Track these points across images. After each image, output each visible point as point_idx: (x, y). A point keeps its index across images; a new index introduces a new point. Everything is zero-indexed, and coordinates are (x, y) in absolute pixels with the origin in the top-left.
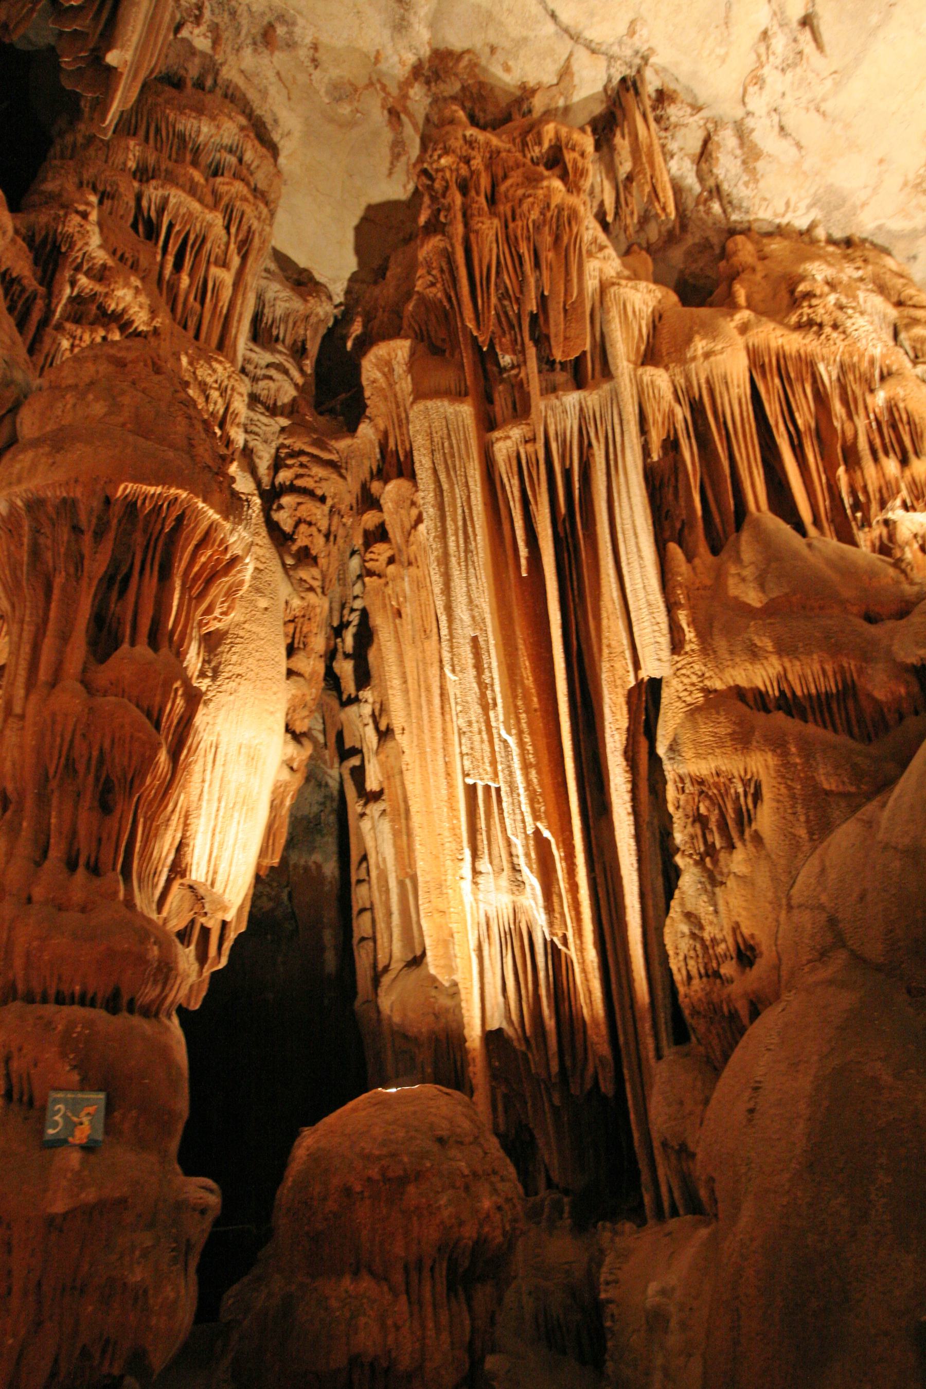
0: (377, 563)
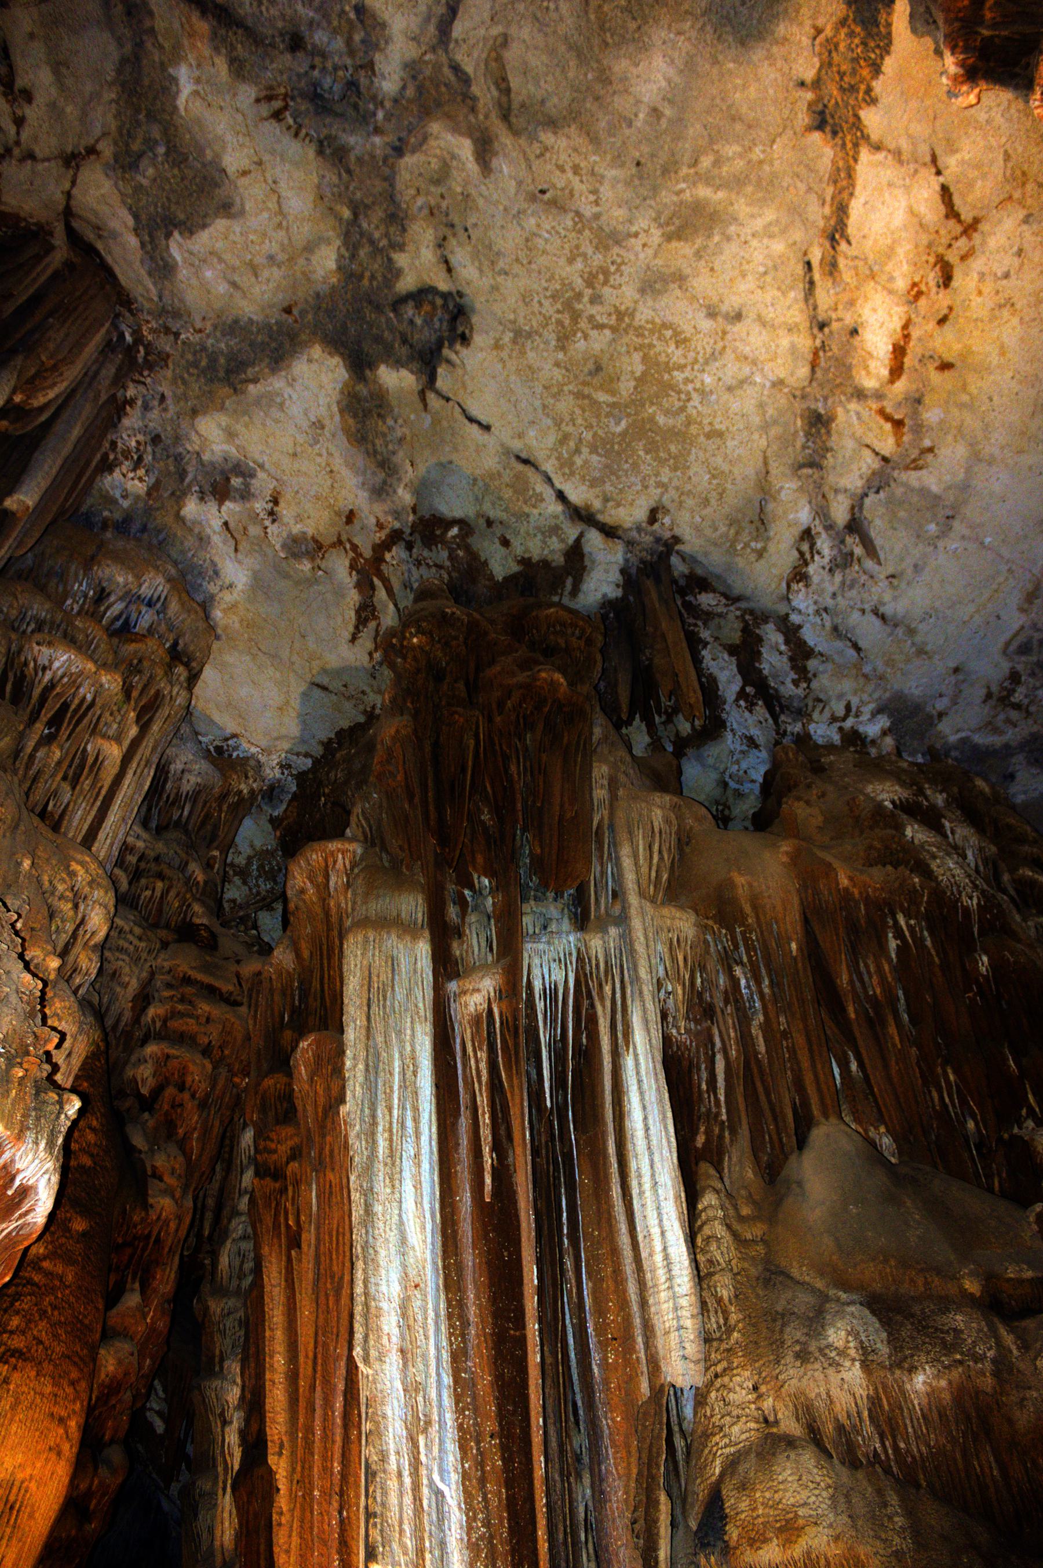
0: (275, 1157)
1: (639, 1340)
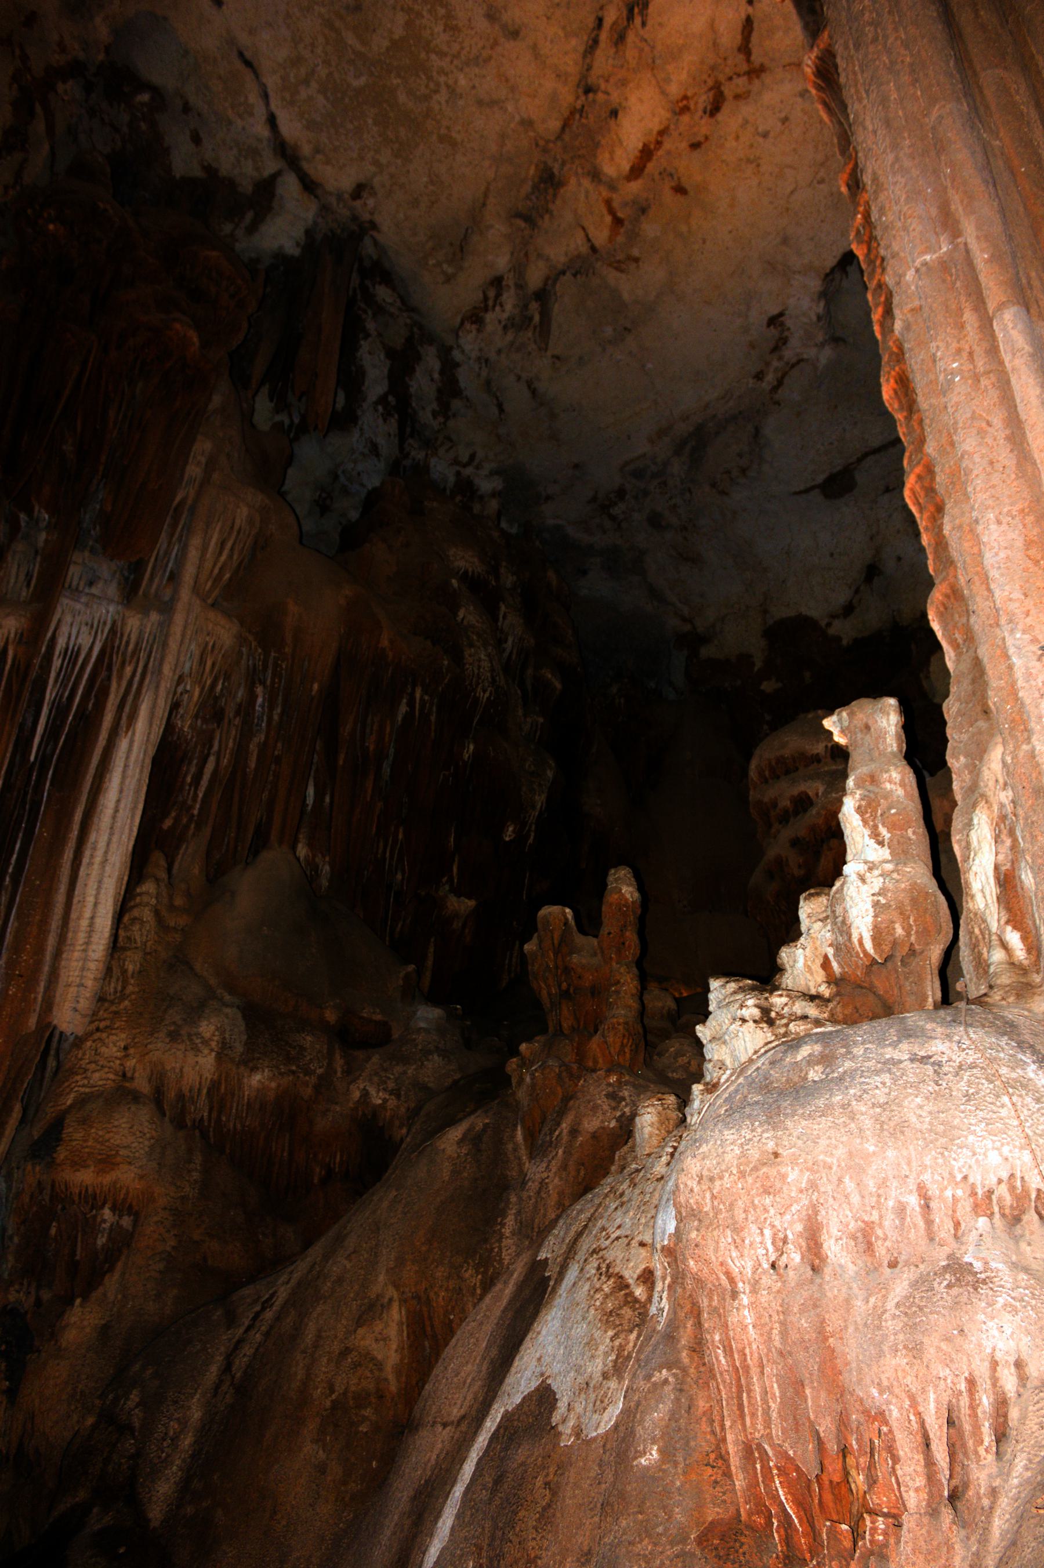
1: (42, 984)
